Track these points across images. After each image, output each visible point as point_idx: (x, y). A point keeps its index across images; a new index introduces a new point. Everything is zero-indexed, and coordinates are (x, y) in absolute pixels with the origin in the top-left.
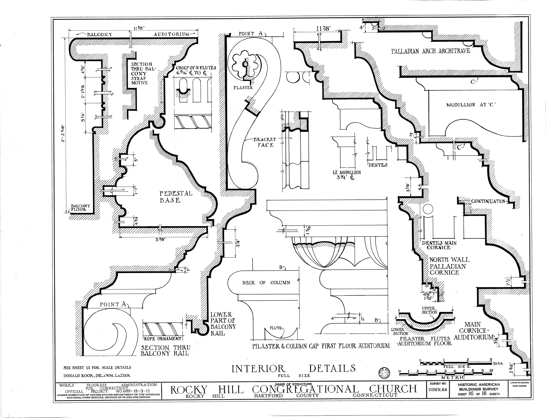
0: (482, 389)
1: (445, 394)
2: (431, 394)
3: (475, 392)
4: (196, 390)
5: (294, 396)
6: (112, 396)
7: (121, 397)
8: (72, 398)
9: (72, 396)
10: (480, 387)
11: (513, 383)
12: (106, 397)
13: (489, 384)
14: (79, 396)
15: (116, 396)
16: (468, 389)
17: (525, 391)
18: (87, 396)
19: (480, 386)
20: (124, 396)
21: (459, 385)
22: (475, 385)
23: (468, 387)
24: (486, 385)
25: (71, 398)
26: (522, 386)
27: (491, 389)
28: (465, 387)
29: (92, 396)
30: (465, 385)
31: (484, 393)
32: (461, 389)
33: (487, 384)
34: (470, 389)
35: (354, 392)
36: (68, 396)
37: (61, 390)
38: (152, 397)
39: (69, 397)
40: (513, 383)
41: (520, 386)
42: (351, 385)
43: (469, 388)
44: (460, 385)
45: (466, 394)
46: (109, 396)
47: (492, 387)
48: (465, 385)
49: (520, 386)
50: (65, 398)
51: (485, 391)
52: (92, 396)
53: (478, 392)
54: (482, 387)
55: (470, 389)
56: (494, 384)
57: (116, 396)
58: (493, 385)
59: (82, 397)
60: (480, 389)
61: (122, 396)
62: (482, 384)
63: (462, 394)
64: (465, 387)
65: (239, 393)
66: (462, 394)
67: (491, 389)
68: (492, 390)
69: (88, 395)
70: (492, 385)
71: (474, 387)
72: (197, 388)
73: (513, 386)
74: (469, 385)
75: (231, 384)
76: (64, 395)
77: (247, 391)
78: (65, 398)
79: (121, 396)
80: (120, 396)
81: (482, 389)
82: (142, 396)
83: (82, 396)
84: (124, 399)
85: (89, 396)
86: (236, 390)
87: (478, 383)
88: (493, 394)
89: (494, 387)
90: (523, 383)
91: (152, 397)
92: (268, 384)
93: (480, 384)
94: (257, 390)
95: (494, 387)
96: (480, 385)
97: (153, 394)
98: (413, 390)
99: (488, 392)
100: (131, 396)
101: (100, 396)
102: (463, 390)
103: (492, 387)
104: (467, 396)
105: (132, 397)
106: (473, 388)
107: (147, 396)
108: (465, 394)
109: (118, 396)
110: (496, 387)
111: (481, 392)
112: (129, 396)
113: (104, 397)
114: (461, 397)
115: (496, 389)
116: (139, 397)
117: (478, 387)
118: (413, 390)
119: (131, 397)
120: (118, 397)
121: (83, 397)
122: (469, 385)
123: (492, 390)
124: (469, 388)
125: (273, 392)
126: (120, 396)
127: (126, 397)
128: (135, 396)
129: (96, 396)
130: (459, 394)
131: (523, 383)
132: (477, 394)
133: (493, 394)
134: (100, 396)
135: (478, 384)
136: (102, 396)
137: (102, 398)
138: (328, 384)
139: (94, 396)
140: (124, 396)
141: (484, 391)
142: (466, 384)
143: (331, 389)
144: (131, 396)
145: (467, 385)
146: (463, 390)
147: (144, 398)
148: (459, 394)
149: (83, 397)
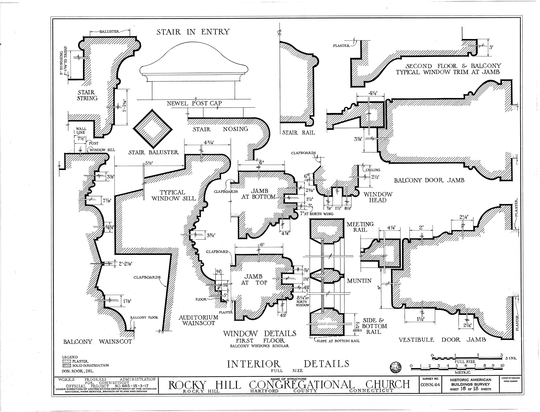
0: (473, 384)
1: (438, 389)
2: (423, 389)
3: (467, 387)
4: (195, 385)
5: (291, 391)
6: (110, 390)
7: (118, 391)
8: (71, 392)
9: (70, 390)
10: (472, 382)
11: (504, 378)
12: (104, 392)
13: (481, 380)
14: (77, 390)
15: (114, 390)
16: (460, 384)
17: (516, 387)
18: (85, 390)
19: (472, 381)
20: (121, 390)
21: (451, 380)
22: (466, 380)
23: (459, 382)
24: (477, 380)
25: (69, 392)
26: (513, 381)
27: (482, 385)
28: (457, 382)
29: (90, 390)
30: (457, 380)
31: (475, 388)
32: (453, 384)
33: (479, 380)
34: (462, 384)
35: (350, 388)
36: (66, 390)
37: (59, 384)
38: (149, 392)
39: (67, 391)
40: (504, 378)
41: (511, 381)
42: (347, 379)
43: (461, 384)
44: (452, 380)
45: (458, 389)
46: (107, 390)
47: (483, 382)
48: (457, 380)
49: (511, 381)
50: (63, 392)
51: (477, 386)
52: (90, 390)
53: (470, 387)
54: (474, 382)
55: (462, 384)
56: (486, 380)
57: (114, 390)
58: (485, 380)
59: (80, 391)
60: (471, 384)
61: (120, 390)
62: (474, 379)
63: (454, 389)
64: (457, 382)
65: (236, 388)
66: (454, 389)
67: (482, 385)
68: (484, 385)
69: (86, 389)
70: (483, 380)
71: (466, 382)
72: (195, 384)
73: (505, 381)
74: (461, 380)
75: (228, 379)
76: (62, 389)
77: (244, 386)
78: (63, 392)
79: (119, 390)
80: (118, 390)
81: (473, 384)
82: (139, 390)
83: (81, 390)
84: (121, 393)
85: (87, 390)
86: (233, 385)
87: (470, 378)
88: (485, 389)
89: (486, 382)
90: (514, 378)
91: (149, 392)
92: (265, 379)
93: (472, 379)
94: (254, 385)
95: (486, 382)
96: (472, 380)
97: (150, 389)
98: (406, 385)
99: (480, 387)
100: (128, 390)
101: (98, 390)
102: (455, 385)
103: (483, 382)
104: (459, 391)
105: (129, 391)
106: (465, 384)
107: (144, 390)
108: (457, 389)
109: (115, 390)
110: (487, 382)
111: (472, 387)
112: (126, 390)
113: (102, 391)
114: (453, 392)
115: (487, 384)
116: (136, 391)
117: (470, 382)
118: (406, 385)
119: (128, 391)
120: (115, 391)
121: (81, 391)
122: (461, 380)
123: (484, 385)
124: (461, 384)
125: (270, 388)
126: (118, 390)
127: (123, 391)
128: (133, 390)
129: (94, 390)
130: (451, 389)
131: (514, 378)
132: (469, 389)
133: (485, 389)
134: (98, 390)
135: (470, 380)
136: (99, 390)
137: (100, 392)
138: (324, 379)
139: (92, 390)
140: (121, 390)
141: (475, 386)
142: (458, 379)
143: (328, 384)
144: (128, 390)
145: (459, 380)
146: (455, 385)
147: (141, 392)
148: (451, 389)
149: (81, 391)
